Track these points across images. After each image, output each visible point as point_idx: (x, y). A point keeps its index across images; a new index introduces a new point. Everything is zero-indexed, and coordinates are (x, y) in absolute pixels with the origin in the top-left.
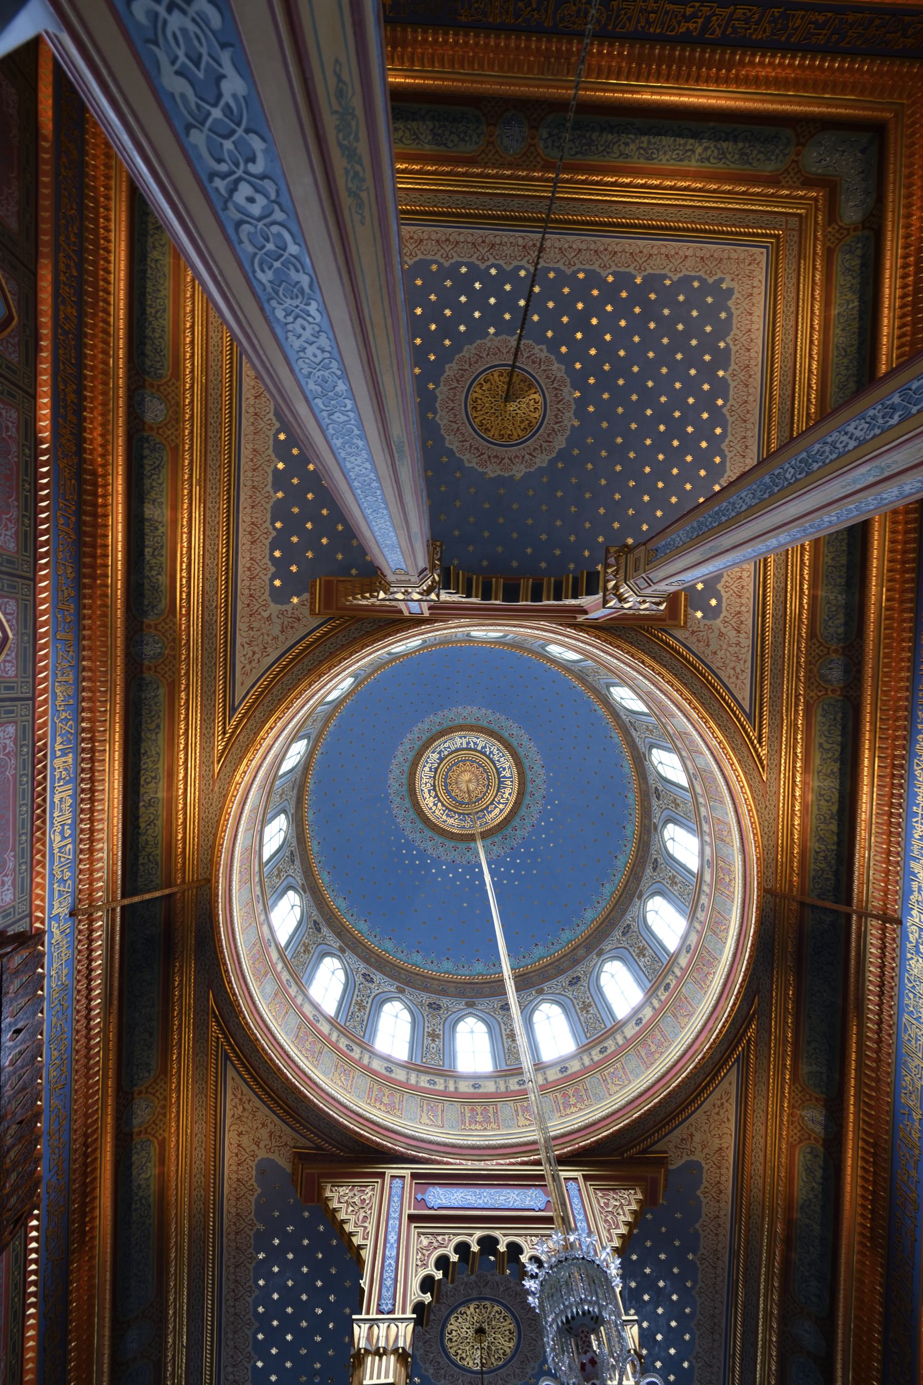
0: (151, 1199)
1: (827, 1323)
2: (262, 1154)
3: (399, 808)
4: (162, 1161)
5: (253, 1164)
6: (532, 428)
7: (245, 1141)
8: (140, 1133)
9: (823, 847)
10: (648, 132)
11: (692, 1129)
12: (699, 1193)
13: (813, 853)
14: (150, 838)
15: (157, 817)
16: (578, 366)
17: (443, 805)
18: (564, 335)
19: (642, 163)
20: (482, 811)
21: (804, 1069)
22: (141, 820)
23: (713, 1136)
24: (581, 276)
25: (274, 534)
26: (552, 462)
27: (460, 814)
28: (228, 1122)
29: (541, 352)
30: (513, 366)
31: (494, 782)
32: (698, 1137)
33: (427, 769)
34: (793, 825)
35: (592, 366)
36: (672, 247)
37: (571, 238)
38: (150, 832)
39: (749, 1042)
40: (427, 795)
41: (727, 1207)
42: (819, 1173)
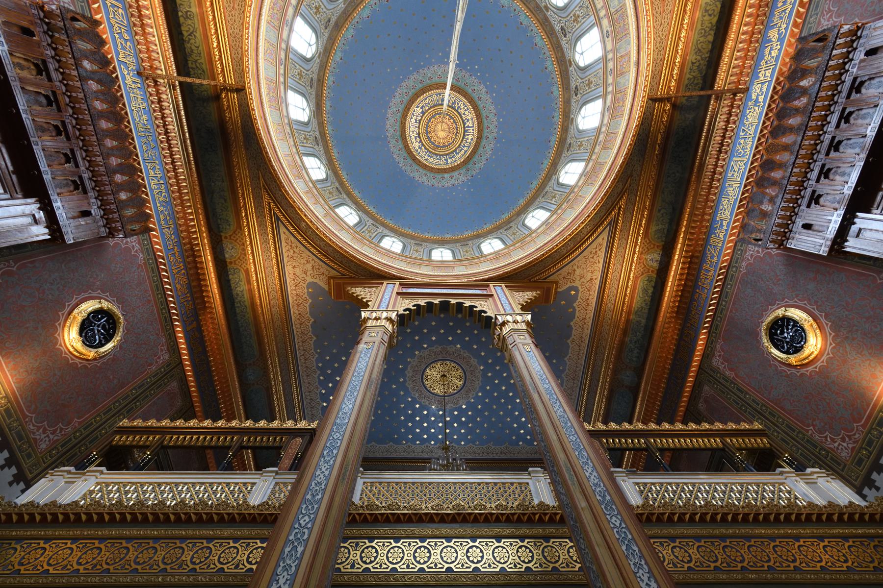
0: (245, 292)
1: (639, 372)
2: (309, 279)
3: (395, 147)
4: (249, 282)
5: (305, 285)
7: (298, 271)
8: (231, 263)
9: (699, 58)
11: (575, 267)
12: (575, 305)
13: (690, 64)
14: (193, 48)
15: (195, 30)
17: (426, 148)
20: (452, 152)
21: (653, 228)
22: (183, 29)
23: (586, 275)
27: (437, 155)
28: (286, 260)
31: (461, 131)
32: (578, 272)
33: (413, 120)
34: (679, 38)
38: (192, 41)
39: (619, 209)
40: (414, 140)
41: (591, 314)
42: (650, 291)
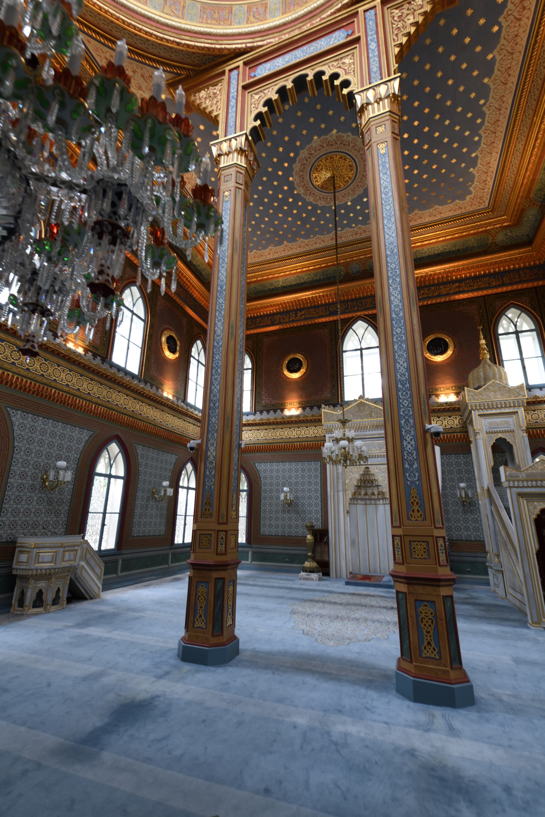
6: (315, 168)
10: (302, 284)
16: (300, 204)
18: (312, 213)
19: (300, 275)
24: (312, 236)
25: (501, 19)
26: (296, 155)
29: (321, 203)
30: (335, 192)
35: (292, 206)
36: (276, 256)
37: (321, 246)
